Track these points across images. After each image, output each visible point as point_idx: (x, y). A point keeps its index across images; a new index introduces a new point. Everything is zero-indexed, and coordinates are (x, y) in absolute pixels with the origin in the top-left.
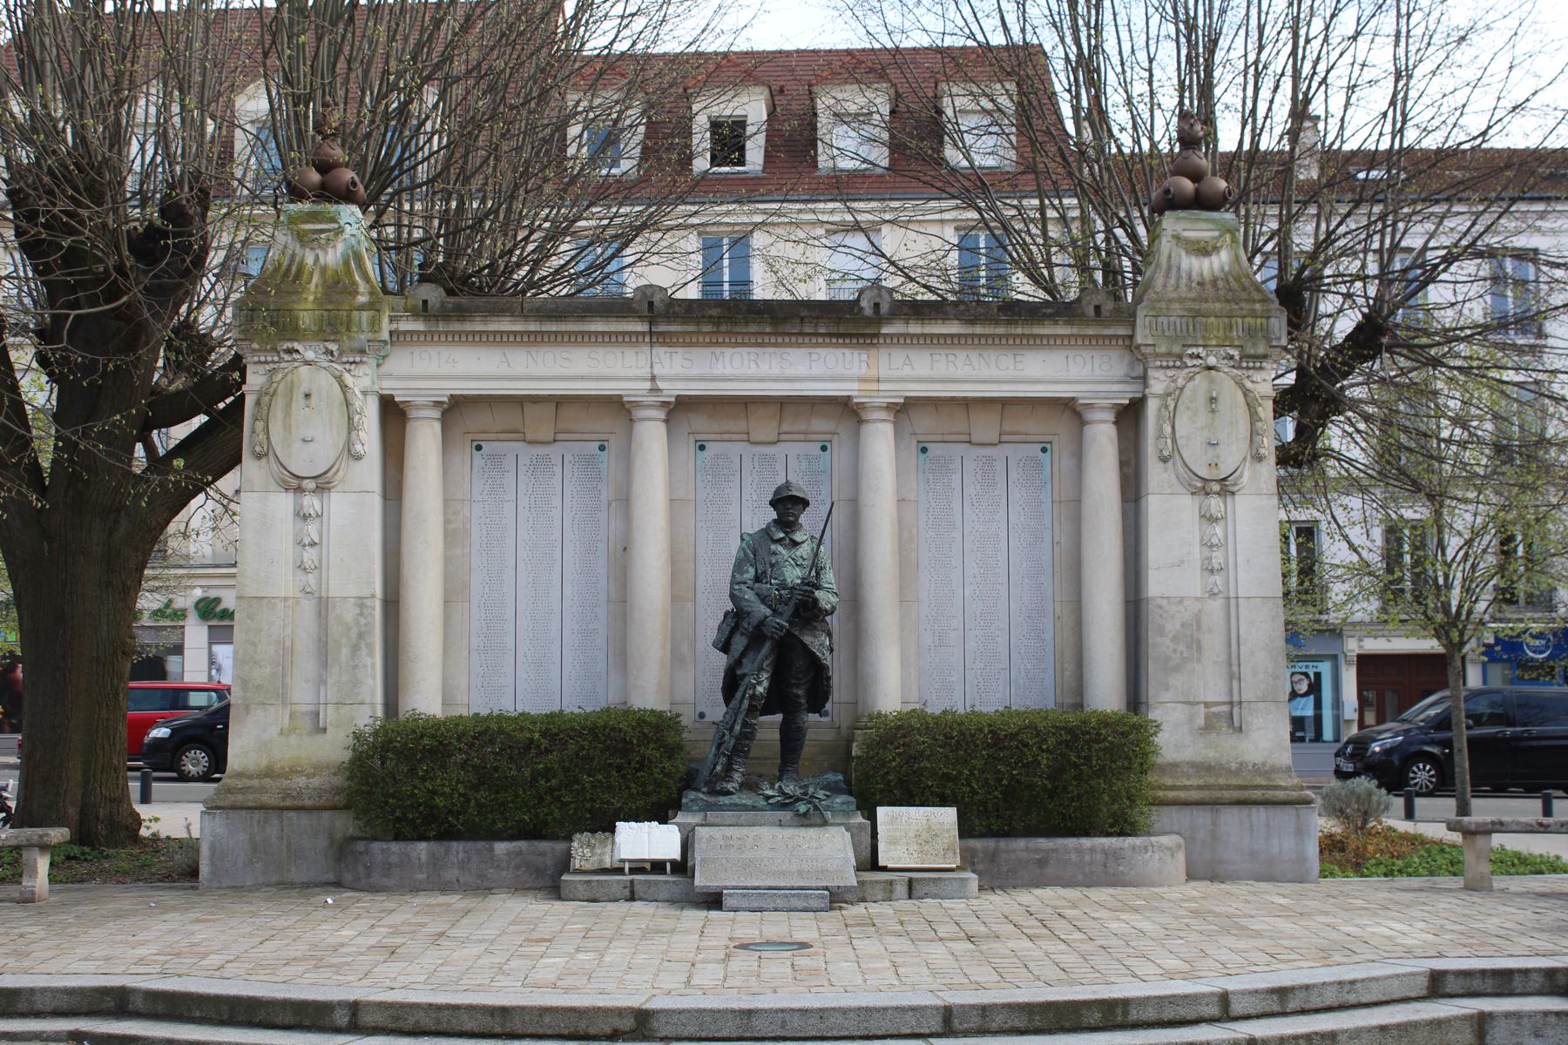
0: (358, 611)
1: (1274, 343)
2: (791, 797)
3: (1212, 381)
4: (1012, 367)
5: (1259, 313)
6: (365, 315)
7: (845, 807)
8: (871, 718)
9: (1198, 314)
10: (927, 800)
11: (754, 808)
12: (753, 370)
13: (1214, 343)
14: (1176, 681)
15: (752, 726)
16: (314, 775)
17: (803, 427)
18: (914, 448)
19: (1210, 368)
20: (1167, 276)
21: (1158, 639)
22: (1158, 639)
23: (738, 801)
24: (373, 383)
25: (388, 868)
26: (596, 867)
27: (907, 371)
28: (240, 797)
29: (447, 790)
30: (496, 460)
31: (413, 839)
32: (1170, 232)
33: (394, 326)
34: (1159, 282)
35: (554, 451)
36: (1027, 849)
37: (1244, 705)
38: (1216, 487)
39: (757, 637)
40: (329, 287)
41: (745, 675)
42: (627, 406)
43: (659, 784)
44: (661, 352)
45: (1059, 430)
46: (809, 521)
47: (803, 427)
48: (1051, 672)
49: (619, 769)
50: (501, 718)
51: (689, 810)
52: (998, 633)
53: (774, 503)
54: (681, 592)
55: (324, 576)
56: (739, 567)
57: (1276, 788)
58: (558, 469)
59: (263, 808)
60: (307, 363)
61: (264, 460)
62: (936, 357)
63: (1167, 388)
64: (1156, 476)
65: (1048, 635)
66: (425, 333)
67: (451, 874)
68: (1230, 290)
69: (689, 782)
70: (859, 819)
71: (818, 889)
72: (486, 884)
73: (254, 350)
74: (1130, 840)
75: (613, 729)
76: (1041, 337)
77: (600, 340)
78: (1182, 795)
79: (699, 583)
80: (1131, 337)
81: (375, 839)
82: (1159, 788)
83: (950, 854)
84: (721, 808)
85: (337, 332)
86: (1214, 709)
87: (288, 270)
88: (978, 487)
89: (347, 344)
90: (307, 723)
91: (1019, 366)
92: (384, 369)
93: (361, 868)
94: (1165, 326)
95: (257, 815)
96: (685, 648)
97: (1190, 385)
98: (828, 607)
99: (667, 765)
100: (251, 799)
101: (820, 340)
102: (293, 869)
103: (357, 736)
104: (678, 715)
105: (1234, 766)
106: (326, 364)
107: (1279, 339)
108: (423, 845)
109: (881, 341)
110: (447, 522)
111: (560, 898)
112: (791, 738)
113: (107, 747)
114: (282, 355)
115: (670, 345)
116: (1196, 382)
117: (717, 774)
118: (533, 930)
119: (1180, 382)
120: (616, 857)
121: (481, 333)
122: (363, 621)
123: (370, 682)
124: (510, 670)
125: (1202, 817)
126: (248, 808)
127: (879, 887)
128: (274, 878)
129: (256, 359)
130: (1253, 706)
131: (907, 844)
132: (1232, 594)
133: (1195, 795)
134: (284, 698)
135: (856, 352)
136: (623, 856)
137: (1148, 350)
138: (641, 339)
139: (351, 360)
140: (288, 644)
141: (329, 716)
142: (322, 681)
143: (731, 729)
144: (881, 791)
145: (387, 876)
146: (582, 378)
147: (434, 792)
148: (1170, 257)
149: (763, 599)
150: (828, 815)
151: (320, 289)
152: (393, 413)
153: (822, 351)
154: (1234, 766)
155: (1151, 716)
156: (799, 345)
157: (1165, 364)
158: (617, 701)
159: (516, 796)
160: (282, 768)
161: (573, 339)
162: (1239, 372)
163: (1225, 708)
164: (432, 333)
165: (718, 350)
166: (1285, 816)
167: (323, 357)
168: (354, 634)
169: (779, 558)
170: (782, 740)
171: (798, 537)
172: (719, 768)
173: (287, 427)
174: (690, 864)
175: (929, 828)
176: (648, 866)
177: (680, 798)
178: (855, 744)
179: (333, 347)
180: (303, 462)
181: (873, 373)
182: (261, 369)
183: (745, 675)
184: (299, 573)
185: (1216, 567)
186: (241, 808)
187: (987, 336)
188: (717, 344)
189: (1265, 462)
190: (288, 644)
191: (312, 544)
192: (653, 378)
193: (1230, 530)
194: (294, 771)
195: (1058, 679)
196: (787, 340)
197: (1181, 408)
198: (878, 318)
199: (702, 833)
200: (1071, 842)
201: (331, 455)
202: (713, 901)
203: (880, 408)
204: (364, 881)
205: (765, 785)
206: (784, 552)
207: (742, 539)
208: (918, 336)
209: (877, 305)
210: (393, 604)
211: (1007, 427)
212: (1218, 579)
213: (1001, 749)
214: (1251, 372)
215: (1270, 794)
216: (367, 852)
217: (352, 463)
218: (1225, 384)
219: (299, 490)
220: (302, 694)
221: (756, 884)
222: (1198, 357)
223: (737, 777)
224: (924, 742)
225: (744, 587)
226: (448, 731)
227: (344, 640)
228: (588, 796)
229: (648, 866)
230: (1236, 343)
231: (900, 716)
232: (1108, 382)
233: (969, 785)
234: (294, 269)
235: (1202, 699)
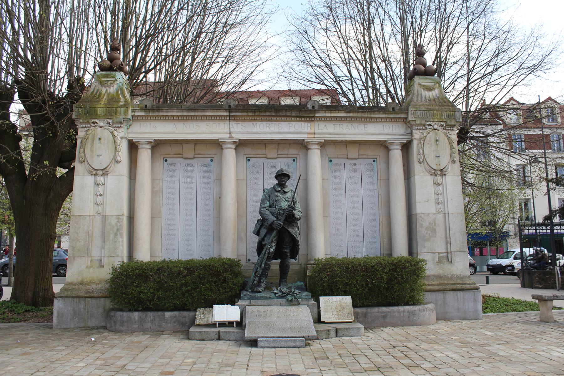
0: (117, 220)
1: (457, 121)
2: (285, 293)
3: (436, 134)
4: (363, 129)
5: (452, 110)
6: (122, 109)
7: (307, 297)
8: (315, 260)
9: (430, 110)
10: (339, 293)
11: (270, 298)
12: (268, 130)
13: (436, 120)
14: (427, 244)
15: (269, 265)
16: (99, 284)
17: (286, 152)
18: (327, 160)
19: (435, 129)
20: (418, 97)
21: (421, 229)
22: (421, 229)
23: (263, 295)
24: (125, 135)
25: (122, 323)
26: (205, 323)
27: (325, 131)
28: (69, 293)
29: (145, 291)
30: (172, 165)
31: (132, 311)
32: (417, 83)
33: (133, 114)
34: (415, 99)
35: (194, 162)
36: (378, 312)
37: (452, 253)
38: (439, 173)
39: (271, 229)
40: (110, 100)
41: (265, 244)
42: (221, 144)
43: (232, 289)
44: (233, 123)
45: (380, 153)
46: (291, 184)
47: (286, 152)
48: (379, 242)
49: (215, 282)
50: (171, 261)
51: (244, 299)
52: (359, 228)
53: (276, 177)
54: (241, 214)
55: (105, 207)
56: (263, 202)
57: (466, 284)
58: (195, 169)
59: (78, 297)
60: (101, 127)
61: (83, 164)
62: (336, 125)
63: (420, 136)
64: (418, 169)
65: (378, 229)
66: (145, 116)
67: (148, 325)
68: (440, 102)
69: (243, 287)
70: (313, 302)
71: (300, 337)
72: (162, 329)
73: (81, 122)
74: (418, 307)
75: (213, 266)
76: (374, 118)
77: (210, 118)
78: (432, 288)
79: (247, 210)
80: (406, 118)
81: (121, 310)
82: (426, 285)
83: (350, 315)
84: (256, 298)
85: (112, 116)
86: (441, 255)
87: (96, 94)
88: (351, 174)
89: (115, 119)
90: (97, 264)
91: (366, 129)
92: (129, 130)
93: (112, 322)
94: (419, 114)
95: (76, 300)
96: (243, 235)
97: (429, 135)
98: (298, 217)
99: (235, 280)
100: (74, 293)
101: (293, 119)
102: (90, 321)
103: (114, 269)
104: (239, 261)
105: (450, 276)
106: (107, 128)
107: (459, 119)
108: (136, 314)
109: (315, 119)
110: (153, 188)
111: (188, 339)
112: (284, 269)
113: (44, 271)
114: (91, 124)
115: (237, 120)
116: (431, 134)
117: (255, 285)
118: (168, 363)
119: (425, 134)
120: (213, 320)
121: (166, 116)
122: (119, 224)
123: (121, 248)
124: (177, 243)
125: (440, 296)
126: (72, 297)
127: (324, 333)
128: (82, 325)
129: (82, 126)
130: (455, 253)
131: (332, 312)
132: (446, 212)
133: (437, 288)
134: (88, 253)
135: (306, 123)
136: (216, 320)
137: (413, 123)
138: (226, 118)
139: (117, 126)
140: (90, 233)
141: (105, 261)
142: (103, 248)
143: (260, 266)
144: (321, 290)
145: (122, 326)
146: (204, 133)
147: (141, 292)
148: (418, 91)
149: (273, 214)
150: (300, 300)
151: (106, 100)
152: (133, 147)
153: (294, 123)
154: (450, 276)
155: (421, 257)
156: (285, 121)
157: (419, 128)
158: (217, 255)
159: (174, 293)
160: (87, 281)
161: (200, 119)
162: (445, 131)
163: (445, 254)
164: (148, 116)
165: (255, 123)
166: (469, 294)
167: (107, 125)
168: (115, 230)
169: (279, 198)
170: (280, 270)
171: (286, 190)
172: (255, 282)
173: (92, 151)
174: (243, 324)
175: (341, 305)
176: (227, 323)
177: (240, 294)
178: (308, 271)
179: (110, 121)
180: (98, 164)
181: (312, 131)
182: (84, 130)
183: (265, 244)
184: (96, 206)
185: (441, 202)
186: (70, 297)
187: (354, 117)
188: (254, 120)
189: (456, 163)
190: (90, 233)
191: (101, 195)
192: (230, 133)
193: (445, 188)
194: (91, 282)
195: (382, 245)
196: (280, 118)
197: (425, 144)
198: (314, 110)
199: (249, 309)
200: (395, 308)
201: (108, 161)
202: (253, 343)
203: (315, 144)
204: (113, 328)
205: (274, 288)
206: (281, 196)
207: (264, 191)
208: (329, 117)
209: (313, 107)
210: (131, 219)
211: (361, 152)
212: (441, 206)
213: (367, 272)
214: (449, 131)
215: (464, 286)
216: (115, 316)
217: (116, 164)
218: (441, 134)
219: (96, 175)
220: (96, 252)
221: (272, 335)
222: (431, 125)
223: (263, 285)
224: (338, 270)
225: (264, 209)
226: (147, 267)
227: (111, 232)
228: (203, 294)
229: (227, 323)
230: (444, 120)
231: (327, 260)
232: (398, 135)
233: (356, 287)
234: (98, 94)
235: (437, 251)
